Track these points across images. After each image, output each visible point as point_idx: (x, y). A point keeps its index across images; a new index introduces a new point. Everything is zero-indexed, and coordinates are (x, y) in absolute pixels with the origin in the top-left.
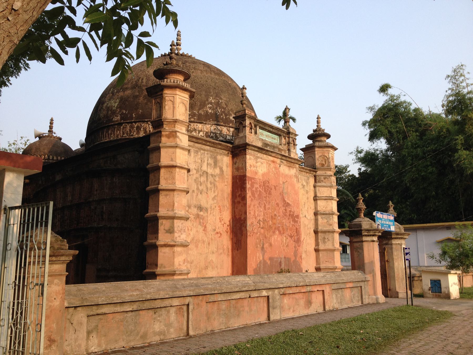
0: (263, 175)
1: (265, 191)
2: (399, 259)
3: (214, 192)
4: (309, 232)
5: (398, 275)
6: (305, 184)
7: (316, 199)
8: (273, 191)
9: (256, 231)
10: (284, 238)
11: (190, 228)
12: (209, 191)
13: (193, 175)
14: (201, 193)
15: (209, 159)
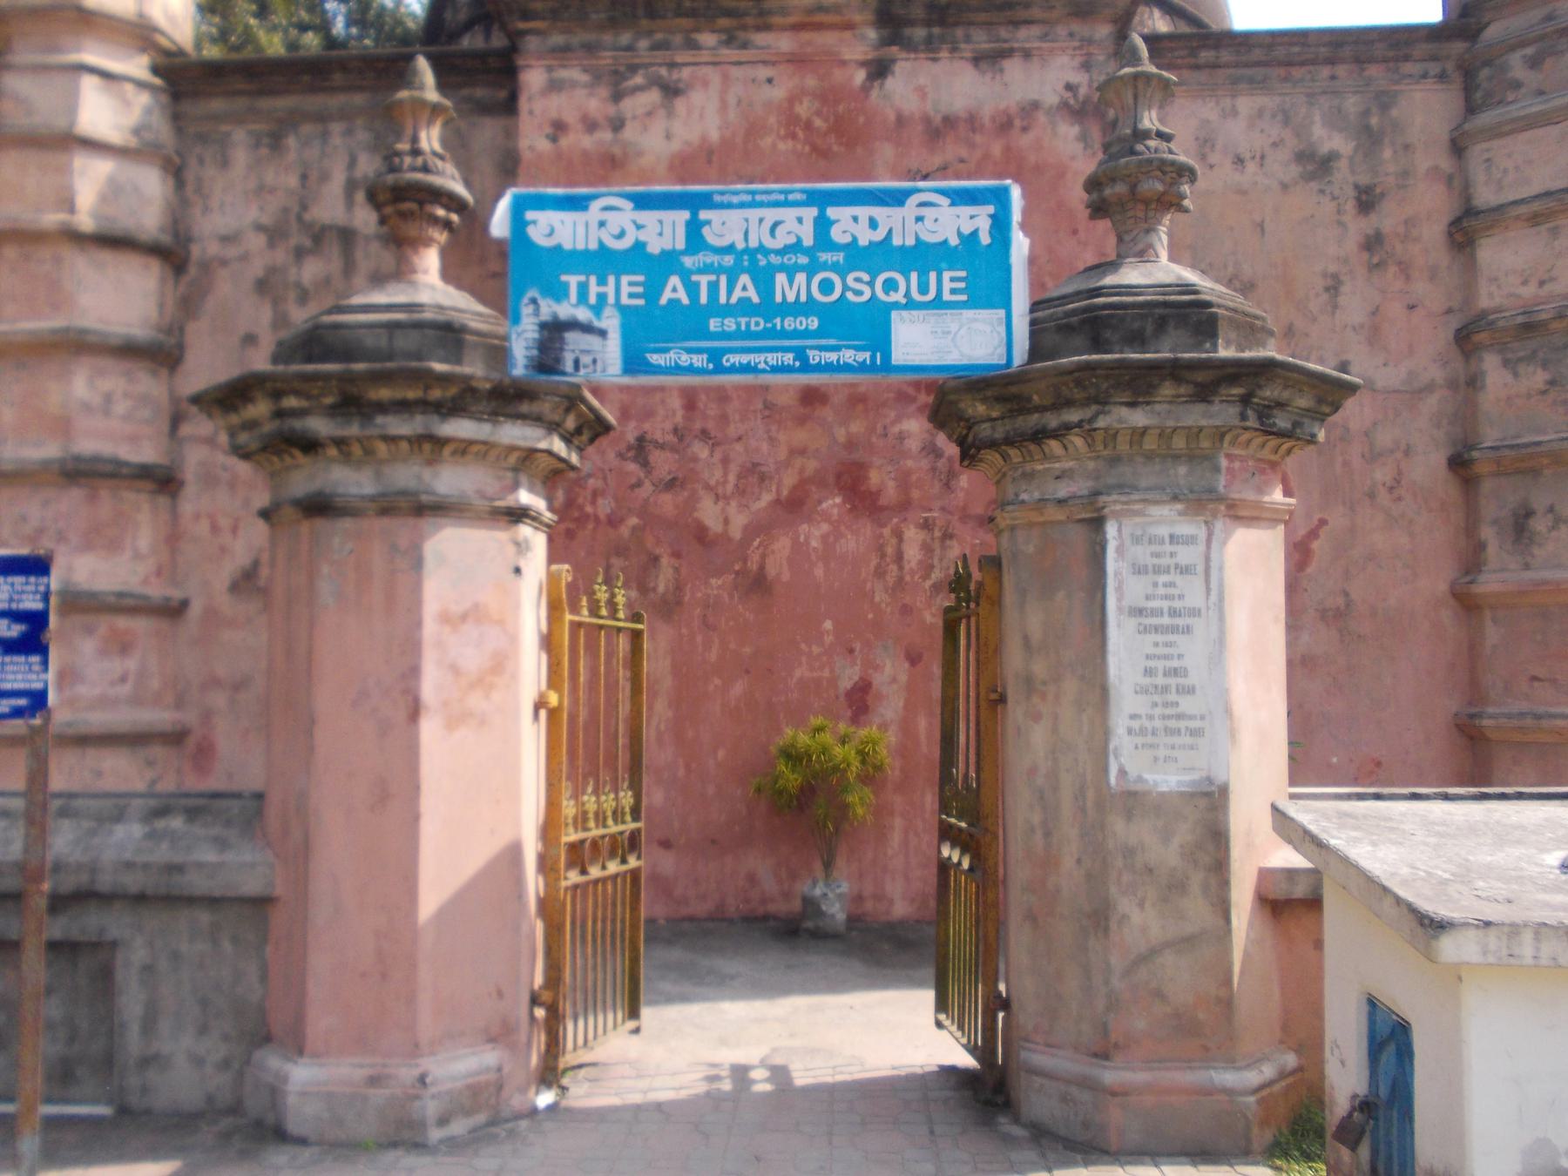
2: (1071, 686)
4: (1382, 474)
5: (1048, 862)
7: (1466, 228)
9: (605, 506)
10: (913, 535)
11: (224, 522)
13: (244, 258)
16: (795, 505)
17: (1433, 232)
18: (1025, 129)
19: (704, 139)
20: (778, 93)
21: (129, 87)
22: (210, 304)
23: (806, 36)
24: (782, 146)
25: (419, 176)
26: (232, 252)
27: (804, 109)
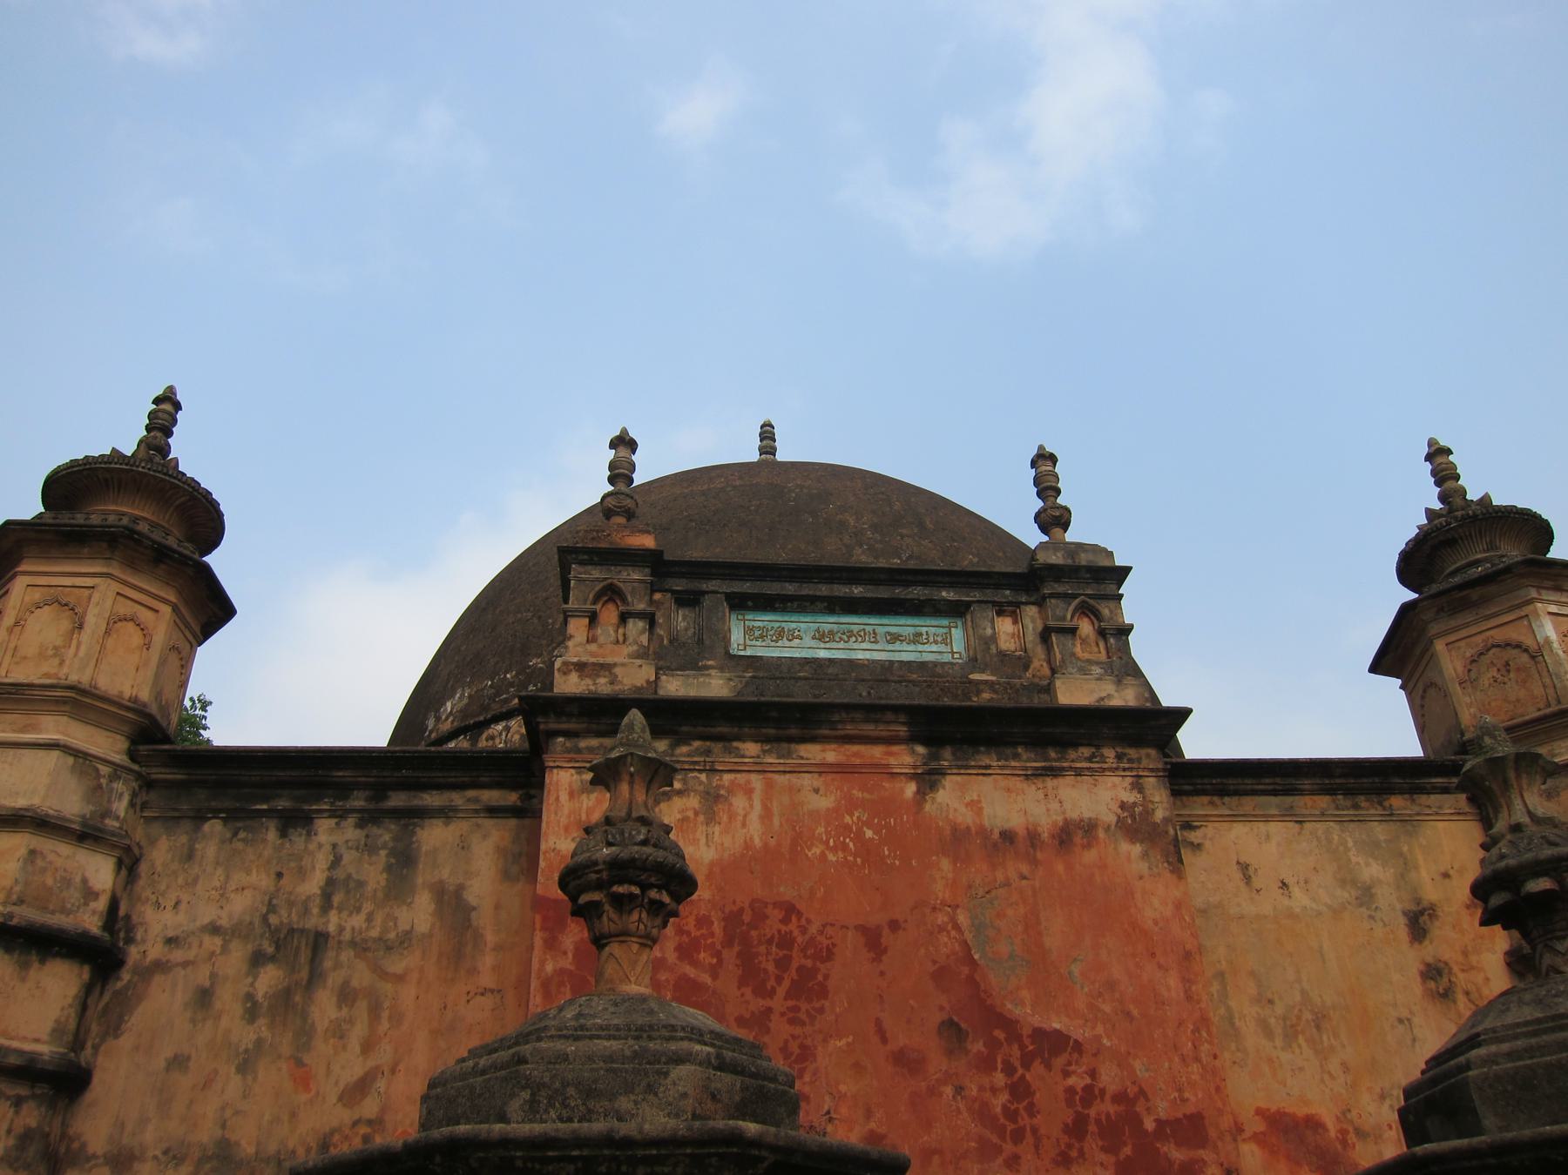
1: (750, 974)
3: (367, 1047)
6: (1372, 870)
14: (245, 1066)
15: (348, 857)
18: (1088, 846)
19: (748, 845)
20: (824, 803)
21: (105, 770)
22: (138, 1020)
23: (855, 748)
24: (831, 857)
25: (648, 850)
26: (178, 955)
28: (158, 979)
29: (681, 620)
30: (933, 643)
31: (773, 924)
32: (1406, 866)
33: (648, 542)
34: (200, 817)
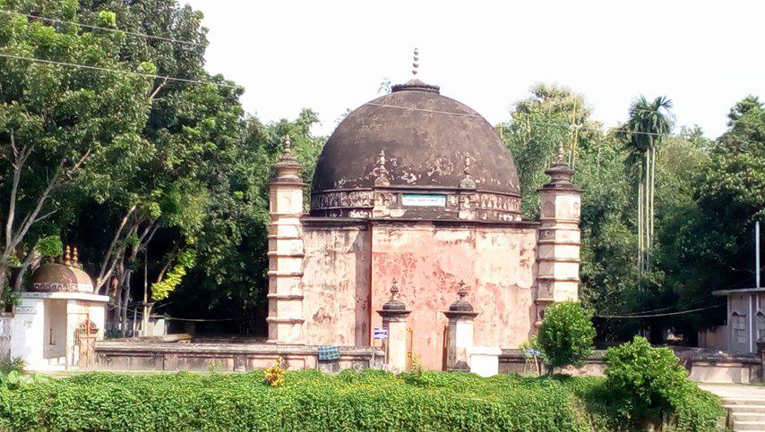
0: (401, 248)
1: (405, 264)
8: (420, 264)
12: (338, 270)
16: (419, 308)
17: (533, 260)
20: (418, 236)
22: (308, 265)
27: (422, 239)
28: (311, 259)
29: (394, 198)
30: (439, 202)
31: (408, 256)
32: (523, 242)
33: (387, 184)
34: (312, 231)
